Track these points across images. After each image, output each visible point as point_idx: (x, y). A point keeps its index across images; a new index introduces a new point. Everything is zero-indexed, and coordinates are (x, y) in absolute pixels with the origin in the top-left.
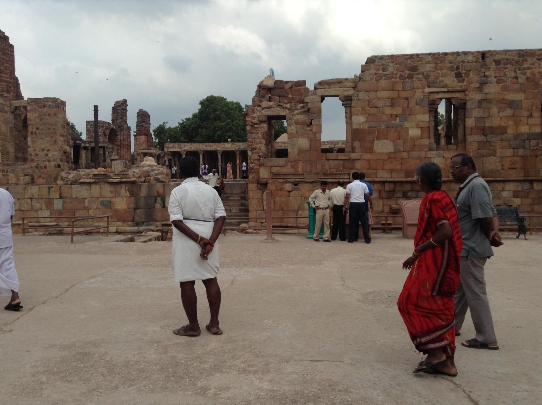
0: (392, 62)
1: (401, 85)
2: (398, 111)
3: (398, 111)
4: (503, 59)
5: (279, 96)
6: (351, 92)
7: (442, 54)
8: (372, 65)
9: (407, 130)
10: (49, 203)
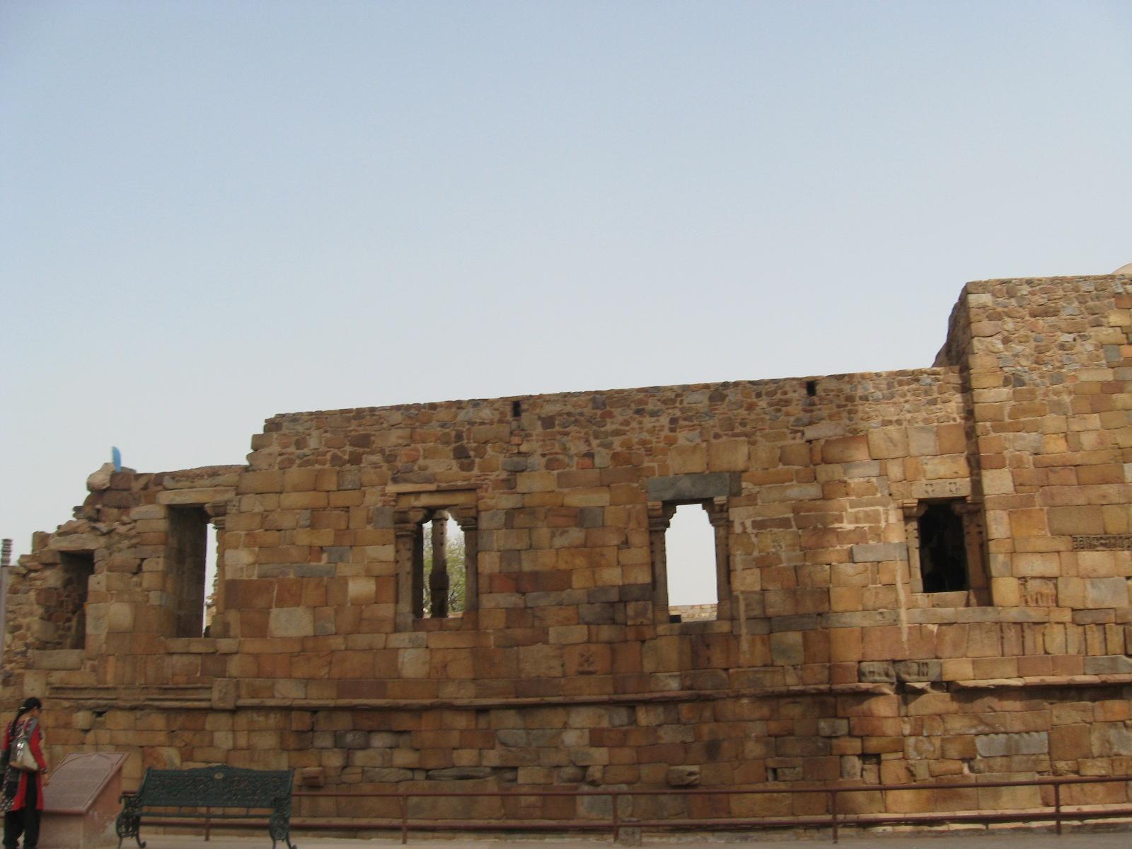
0: (318, 428)
1: (334, 479)
2: (325, 537)
3: (325, 537)
4: (560, 414)
5: (119, 508)
6: (230, 495)
7: (425, 406)
8: (275, 435)
9: (344, 581)
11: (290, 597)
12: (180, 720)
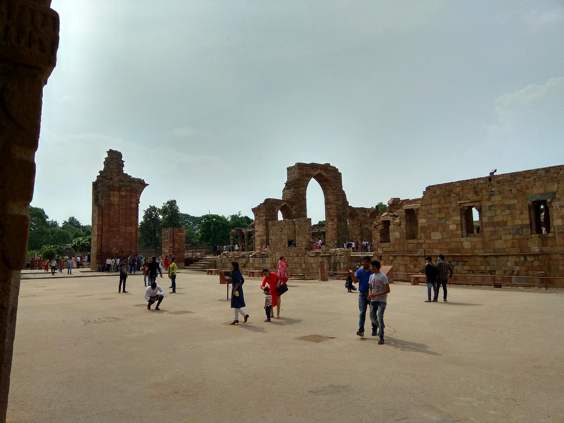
2: (443, 215)
3: (443, 215)
4: (502, 180)
10: (301, 265)
11: (435, 229)
12: (412, 259)
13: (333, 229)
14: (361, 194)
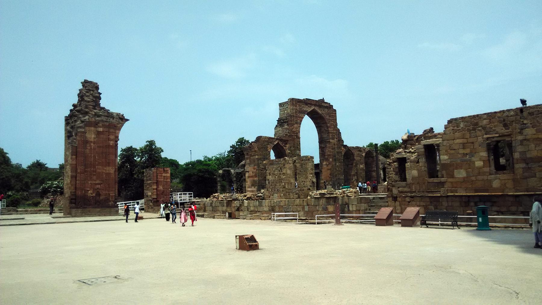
2: (468, 151)
3: (468, 151)
4: (536, 111)
9: (474, 163)
10: (303, 208)
13: (328, 169)
14: (356, 133)
